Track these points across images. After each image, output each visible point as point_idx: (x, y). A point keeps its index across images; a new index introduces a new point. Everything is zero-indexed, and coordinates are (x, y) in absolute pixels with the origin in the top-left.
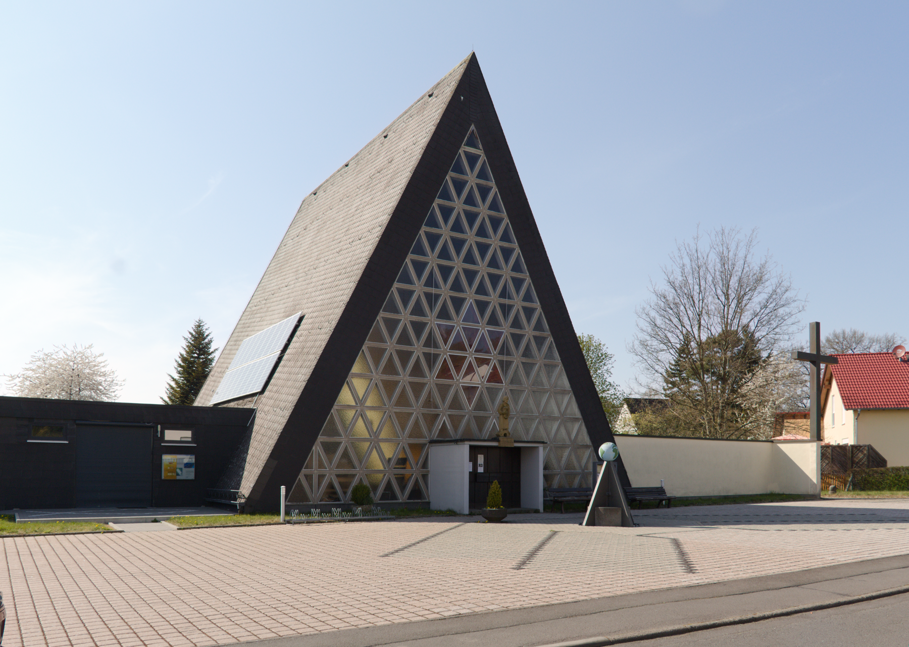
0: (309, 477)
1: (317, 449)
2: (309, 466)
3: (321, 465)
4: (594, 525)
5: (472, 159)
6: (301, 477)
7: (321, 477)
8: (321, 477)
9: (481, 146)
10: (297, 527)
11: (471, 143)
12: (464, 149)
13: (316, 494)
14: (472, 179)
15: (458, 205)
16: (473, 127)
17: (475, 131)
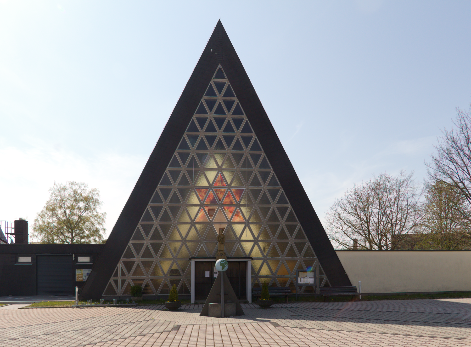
0: (116, 282)
1: (120, 265)
2: (116, 275)
3: (123, 274)
4: (207, 315)
5: (220, 86)
6: (111, 281)
7: (123, 281)
8: (123, 281)
9: (226, 76)
10: (87, 309)
11: (220, 75)
12: (214, 80)
13: (120, 291)
14: (220, 98)
15: (211, 116)
16: (220, 66)
17: (221, 68)
